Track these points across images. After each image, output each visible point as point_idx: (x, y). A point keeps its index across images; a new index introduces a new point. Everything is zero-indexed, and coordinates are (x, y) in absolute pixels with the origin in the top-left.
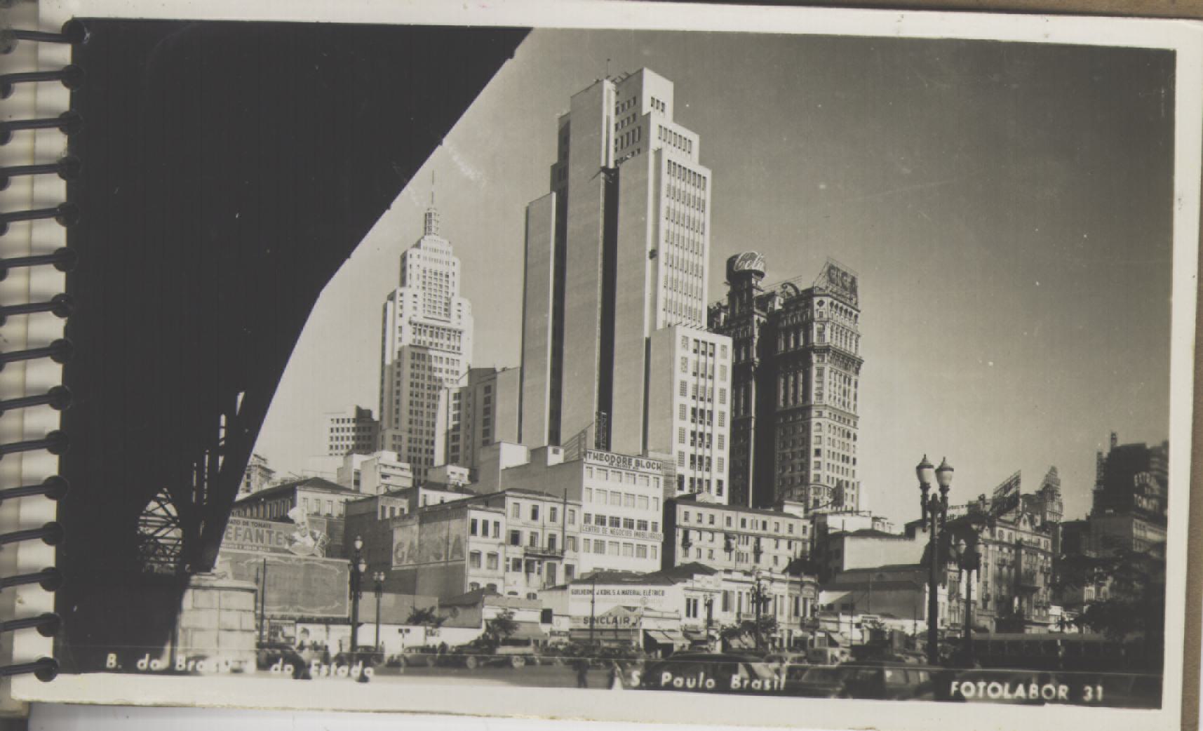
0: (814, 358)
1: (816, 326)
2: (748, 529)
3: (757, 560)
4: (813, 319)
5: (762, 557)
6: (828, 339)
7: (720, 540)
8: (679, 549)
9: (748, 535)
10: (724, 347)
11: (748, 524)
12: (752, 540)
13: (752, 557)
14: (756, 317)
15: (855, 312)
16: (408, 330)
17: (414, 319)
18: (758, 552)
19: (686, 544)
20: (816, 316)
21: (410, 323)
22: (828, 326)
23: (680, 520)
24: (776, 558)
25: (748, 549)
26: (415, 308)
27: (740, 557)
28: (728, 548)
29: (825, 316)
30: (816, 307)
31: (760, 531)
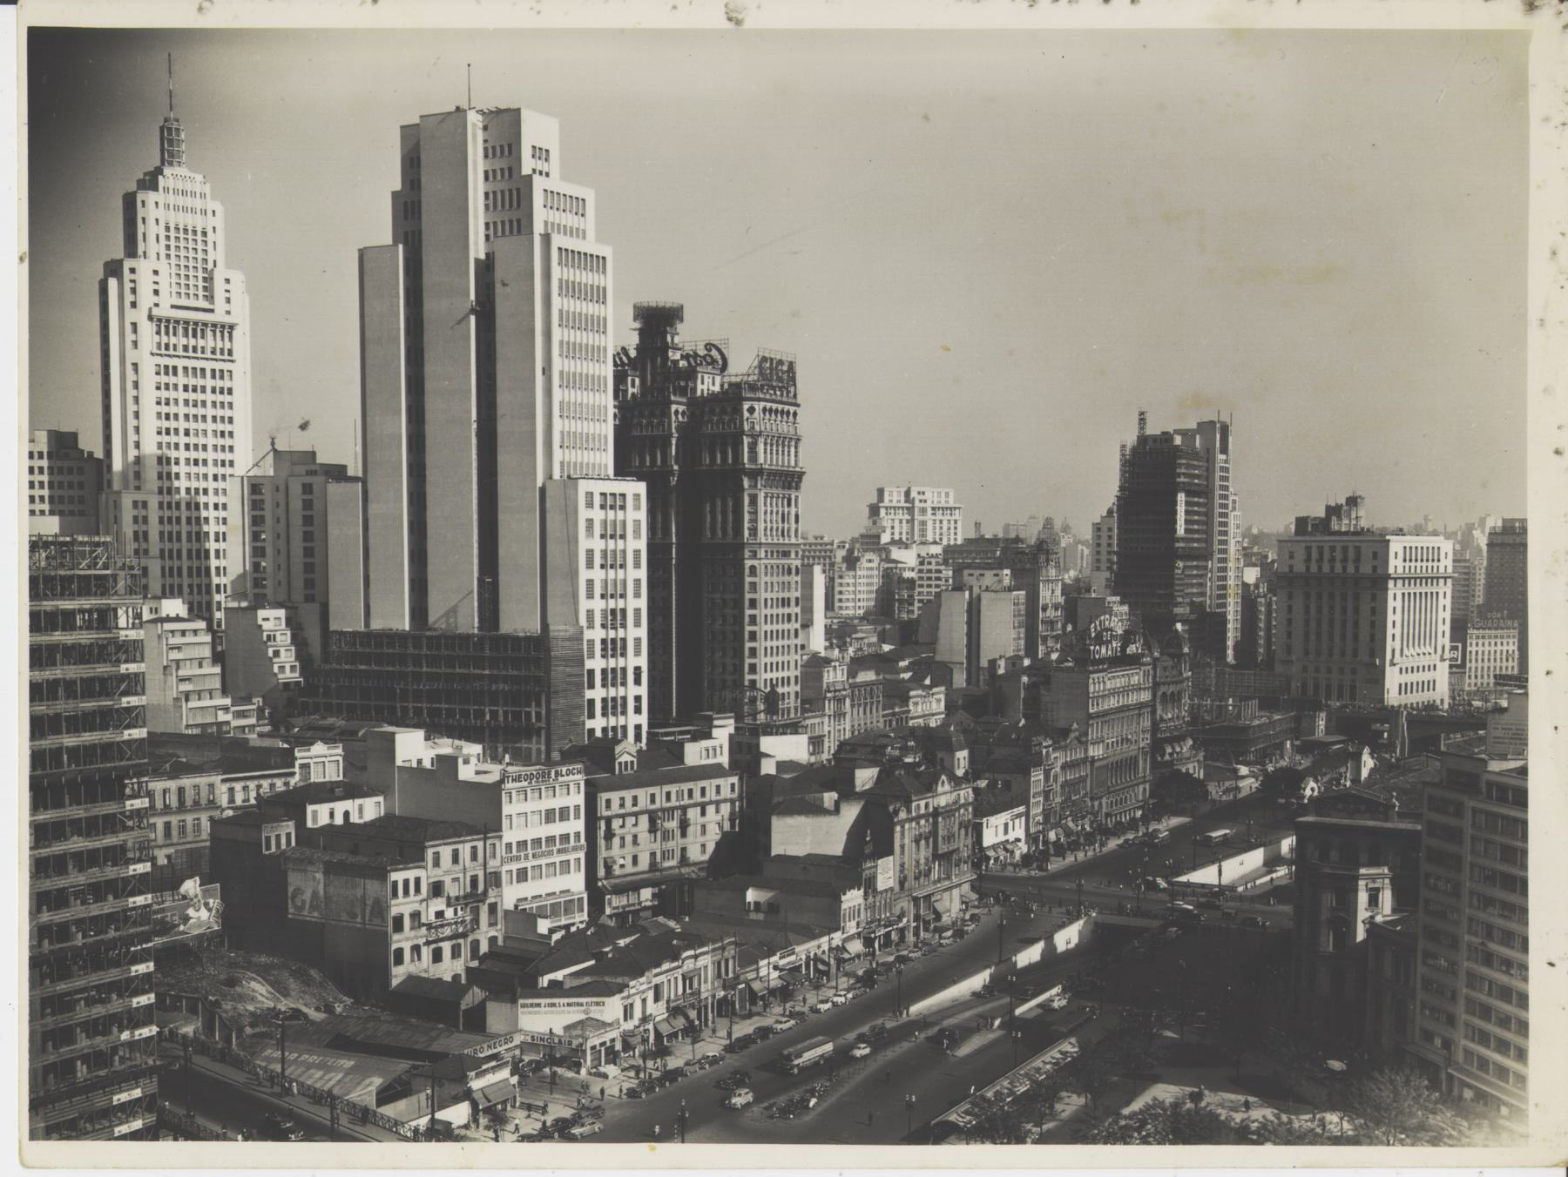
0: (746, 483)
1: (746, 440)
2: (673, 803)
3: (684, 835)
4: (742, 433)
5: (690, 830)
6: (761, 459)
7: (644, 821)
8: (602, 843)
9: (673, 809)
10: (637, 496)
11: (673, 797)
12: (677, 814)
13: (678, 833)
14: (674, 407)
15: (792, 409)
16: (147, 329)
17: (156, 312)
18: (684, 826)
19: (609, 835)
20: (746, 427)
21: (150, 318)
22: (761, 440)
23: (603, 812)
24: (704, 827)
25: (673, 825)
26: (156, 292)
27: (667, 835)
28: (653, 829)
29: (757, 428)
30: (746, 414)
31: (686, 801)
